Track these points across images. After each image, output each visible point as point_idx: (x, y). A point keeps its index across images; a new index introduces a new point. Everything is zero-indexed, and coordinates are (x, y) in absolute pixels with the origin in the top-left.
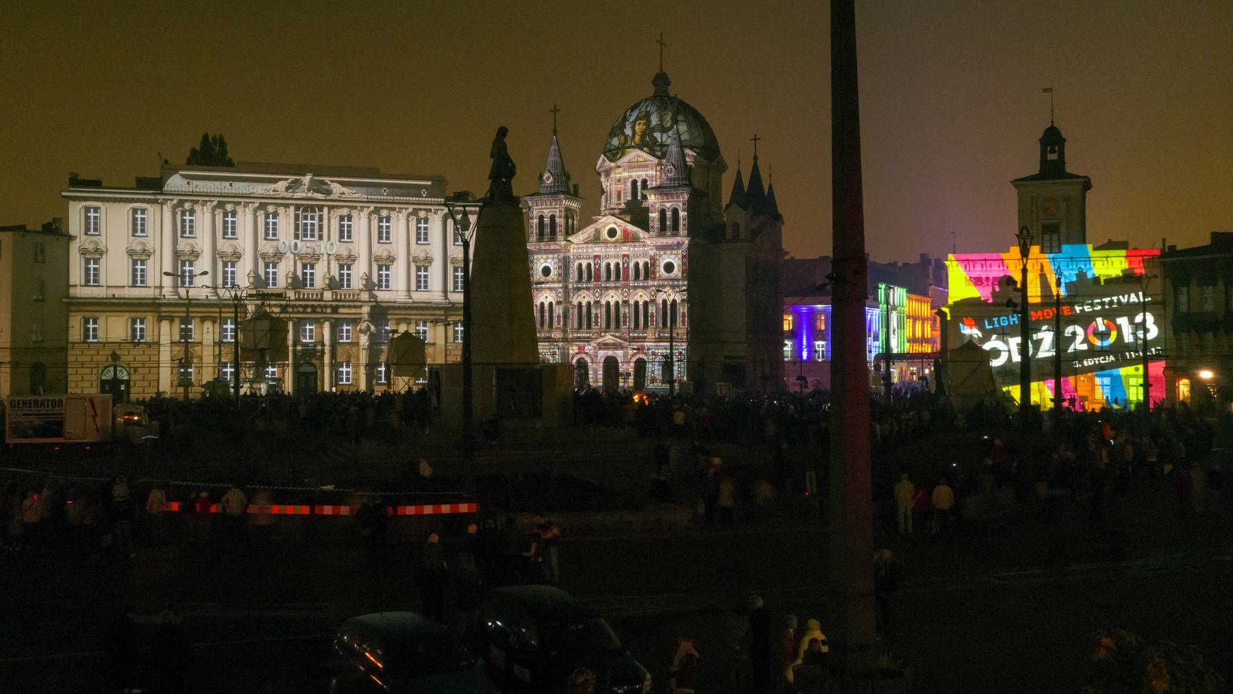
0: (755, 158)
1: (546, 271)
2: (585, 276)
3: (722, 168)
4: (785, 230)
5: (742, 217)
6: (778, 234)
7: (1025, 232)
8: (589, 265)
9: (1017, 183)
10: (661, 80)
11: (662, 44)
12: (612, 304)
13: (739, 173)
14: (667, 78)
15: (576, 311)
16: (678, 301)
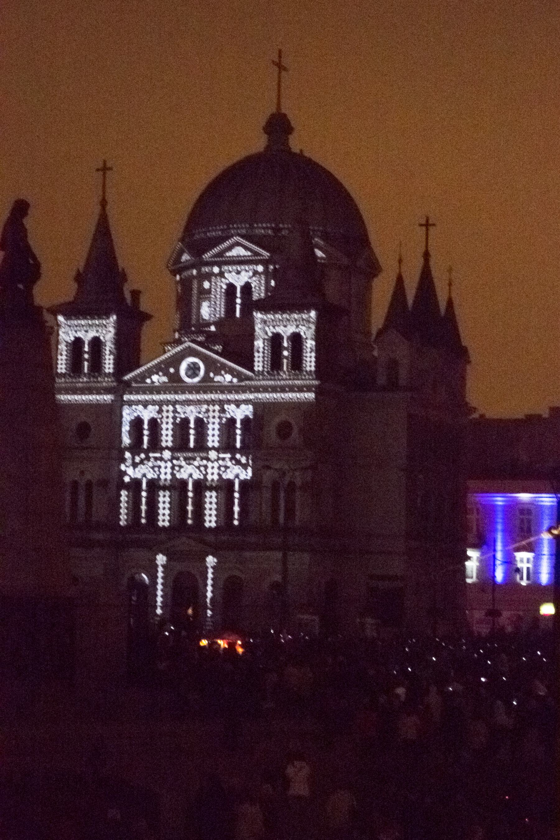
0: (427, 255)
3: (373, 269)
5: (402, 351)
11: (280, 67)
13: (400, 280)
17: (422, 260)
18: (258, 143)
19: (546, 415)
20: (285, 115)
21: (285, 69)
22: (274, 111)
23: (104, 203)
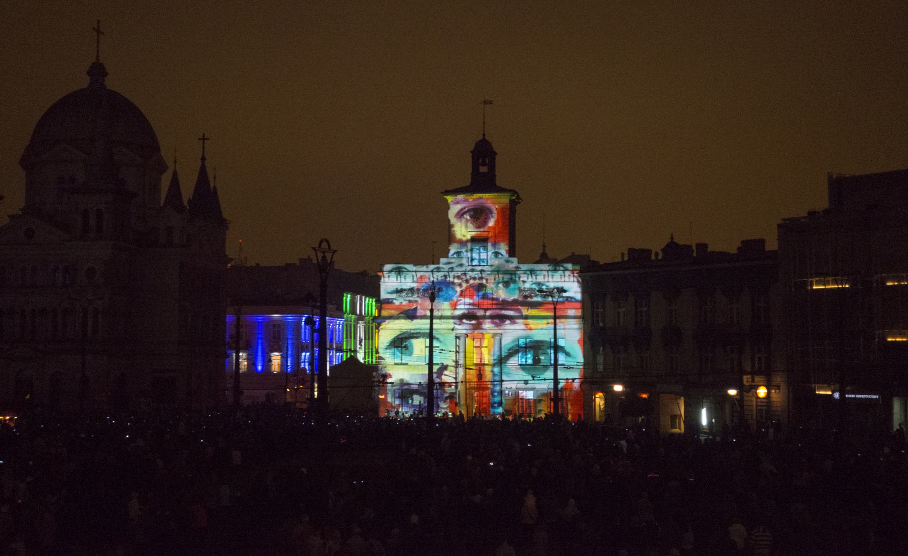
3: (163, 168)
6: (224, 240)
10: (97, 71)
11: (99, 32)
13: (175, 174)
17: (199, 163)
18: (84, 82)
20: (101, 64)
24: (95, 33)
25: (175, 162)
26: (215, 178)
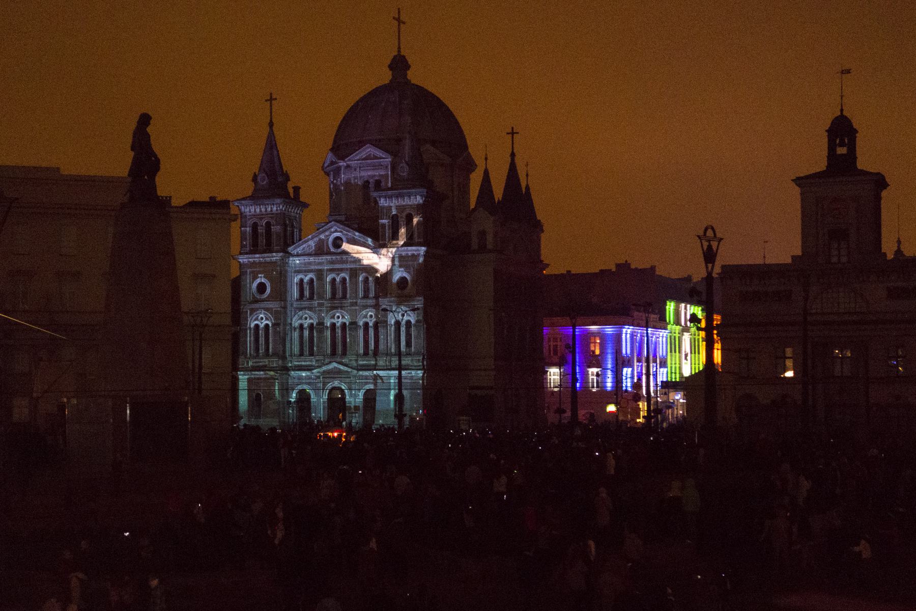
0: (513, 155)
1: (262, 288)
2: (307, 293)
3: (470, 166)
4: (544, 237)
5: (487, 223)
7: (710, 233)
8: (344, 279)
9: (799, 181)
10: (399, 64)
12: (338, 325)
13: (486, 172)
14: (406, 61)
15: (296, 335)
16: (413, 321)
19: (614, 270)
20: (404, 57)
21: (404, 23)
22: (396, 53)
23: (271, 124)
24: (396, 23)
25: (486, 159)
26: (527, 175)
